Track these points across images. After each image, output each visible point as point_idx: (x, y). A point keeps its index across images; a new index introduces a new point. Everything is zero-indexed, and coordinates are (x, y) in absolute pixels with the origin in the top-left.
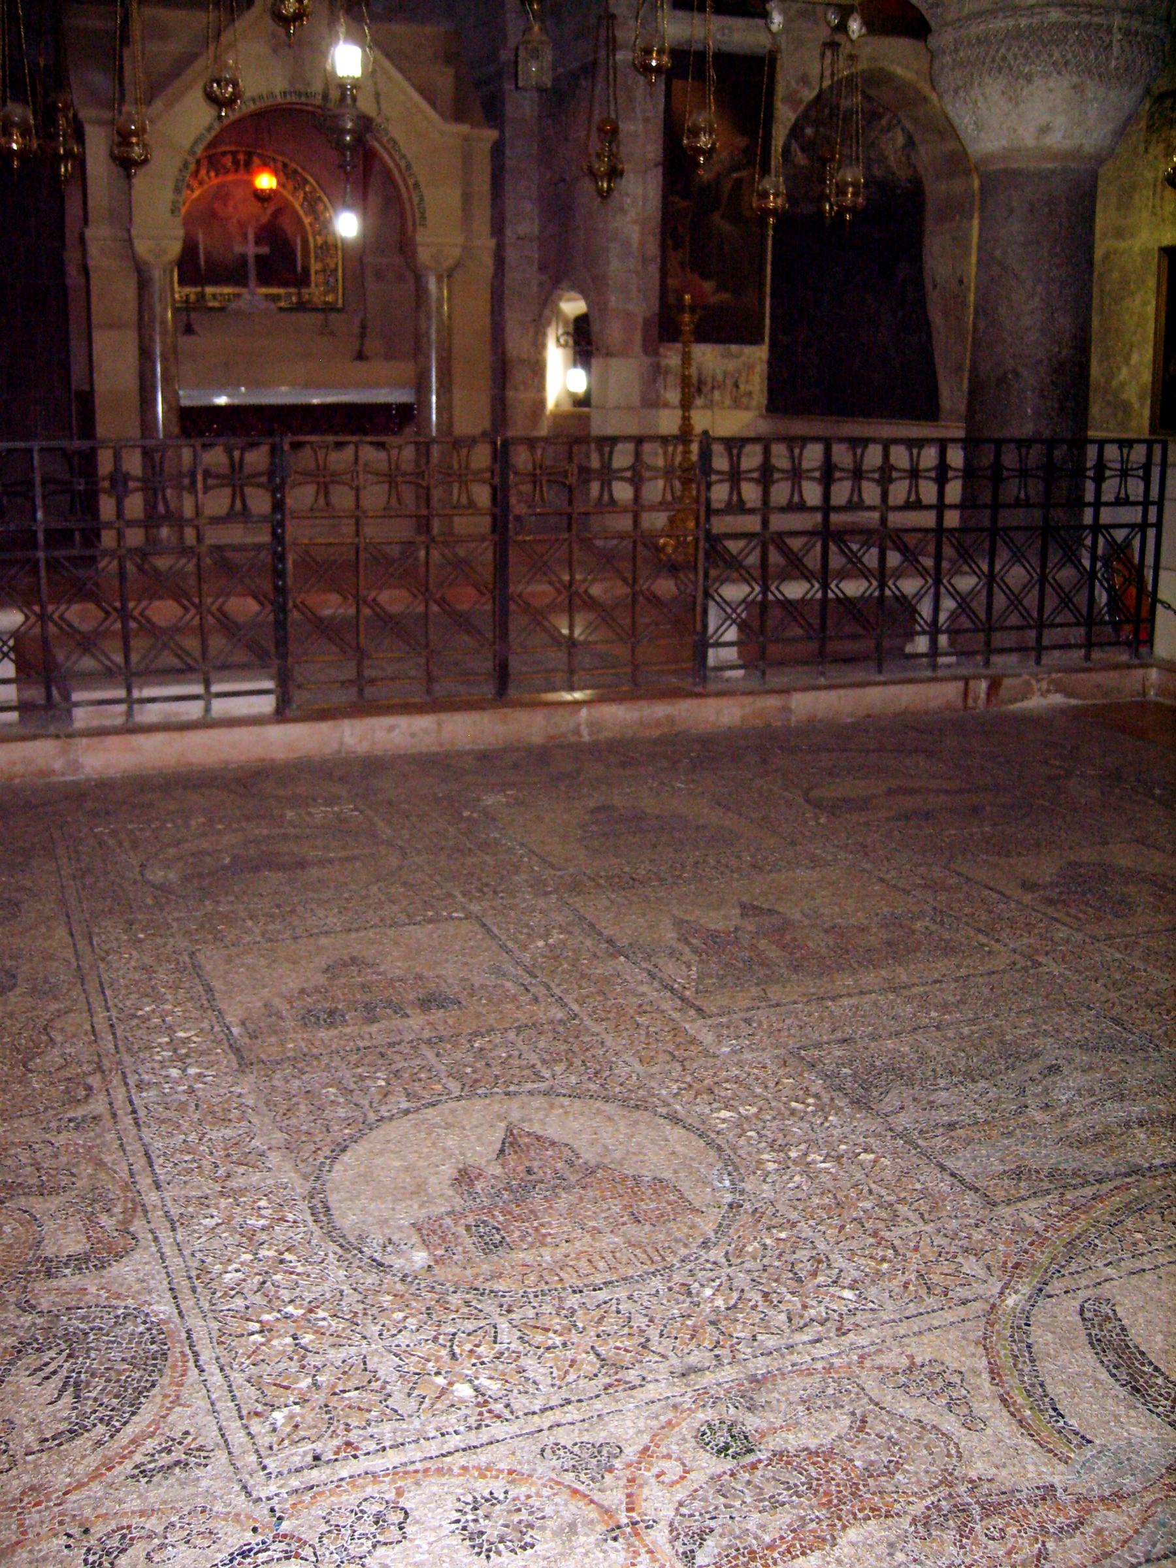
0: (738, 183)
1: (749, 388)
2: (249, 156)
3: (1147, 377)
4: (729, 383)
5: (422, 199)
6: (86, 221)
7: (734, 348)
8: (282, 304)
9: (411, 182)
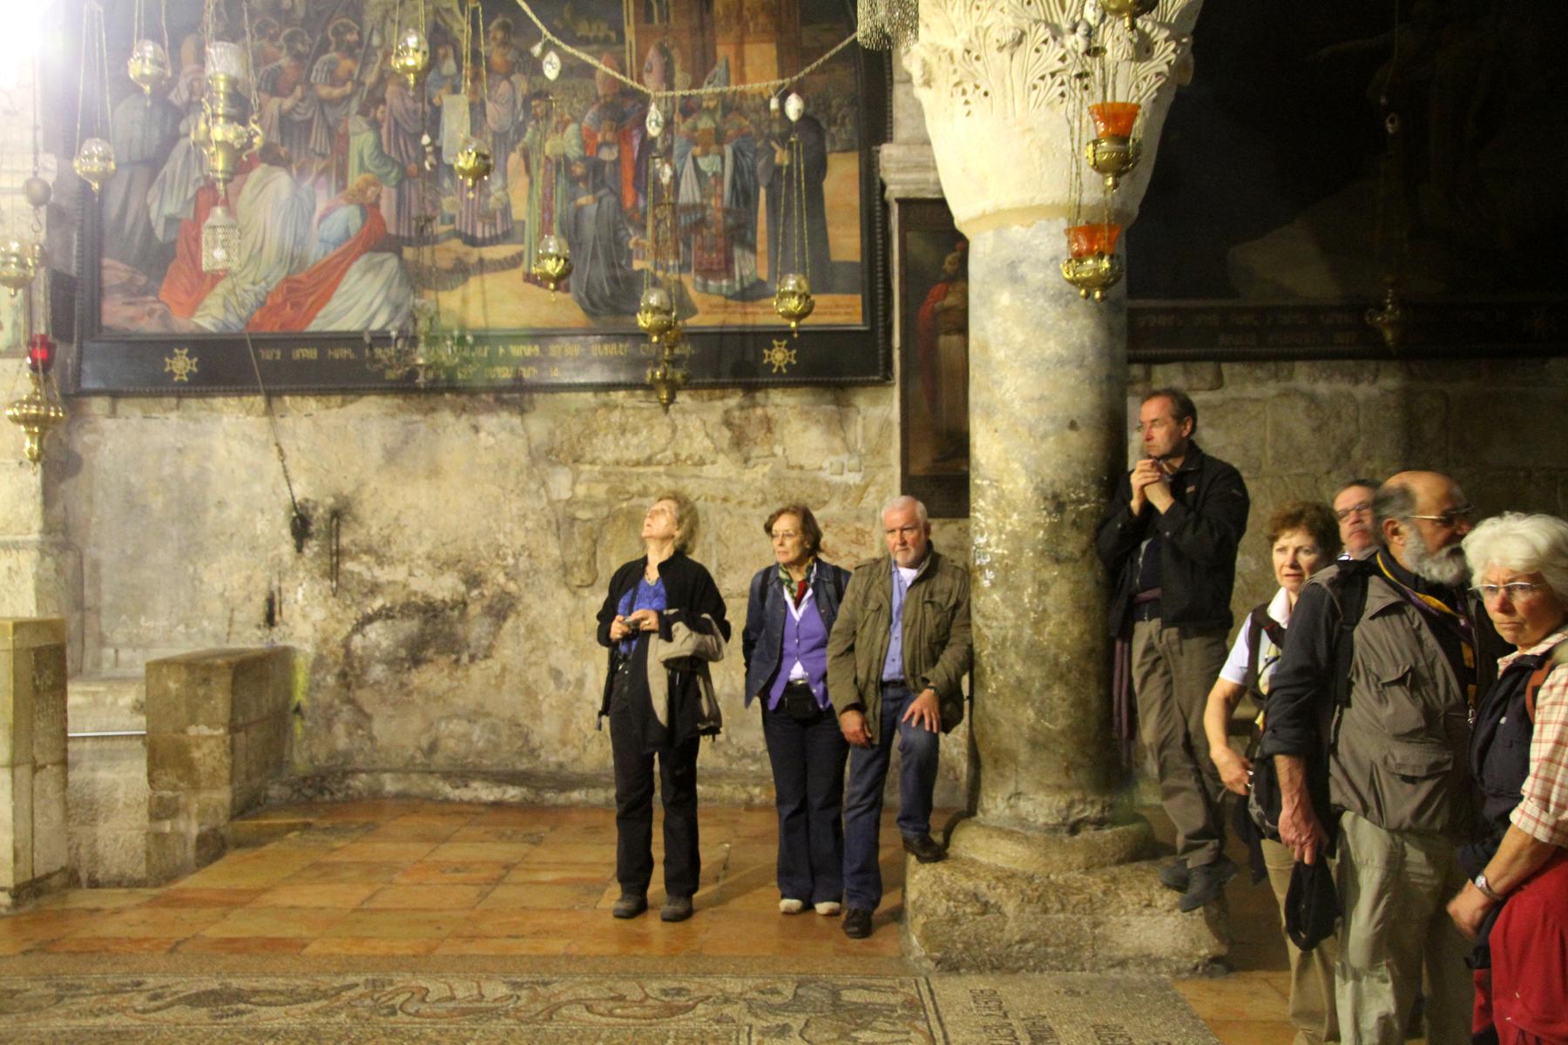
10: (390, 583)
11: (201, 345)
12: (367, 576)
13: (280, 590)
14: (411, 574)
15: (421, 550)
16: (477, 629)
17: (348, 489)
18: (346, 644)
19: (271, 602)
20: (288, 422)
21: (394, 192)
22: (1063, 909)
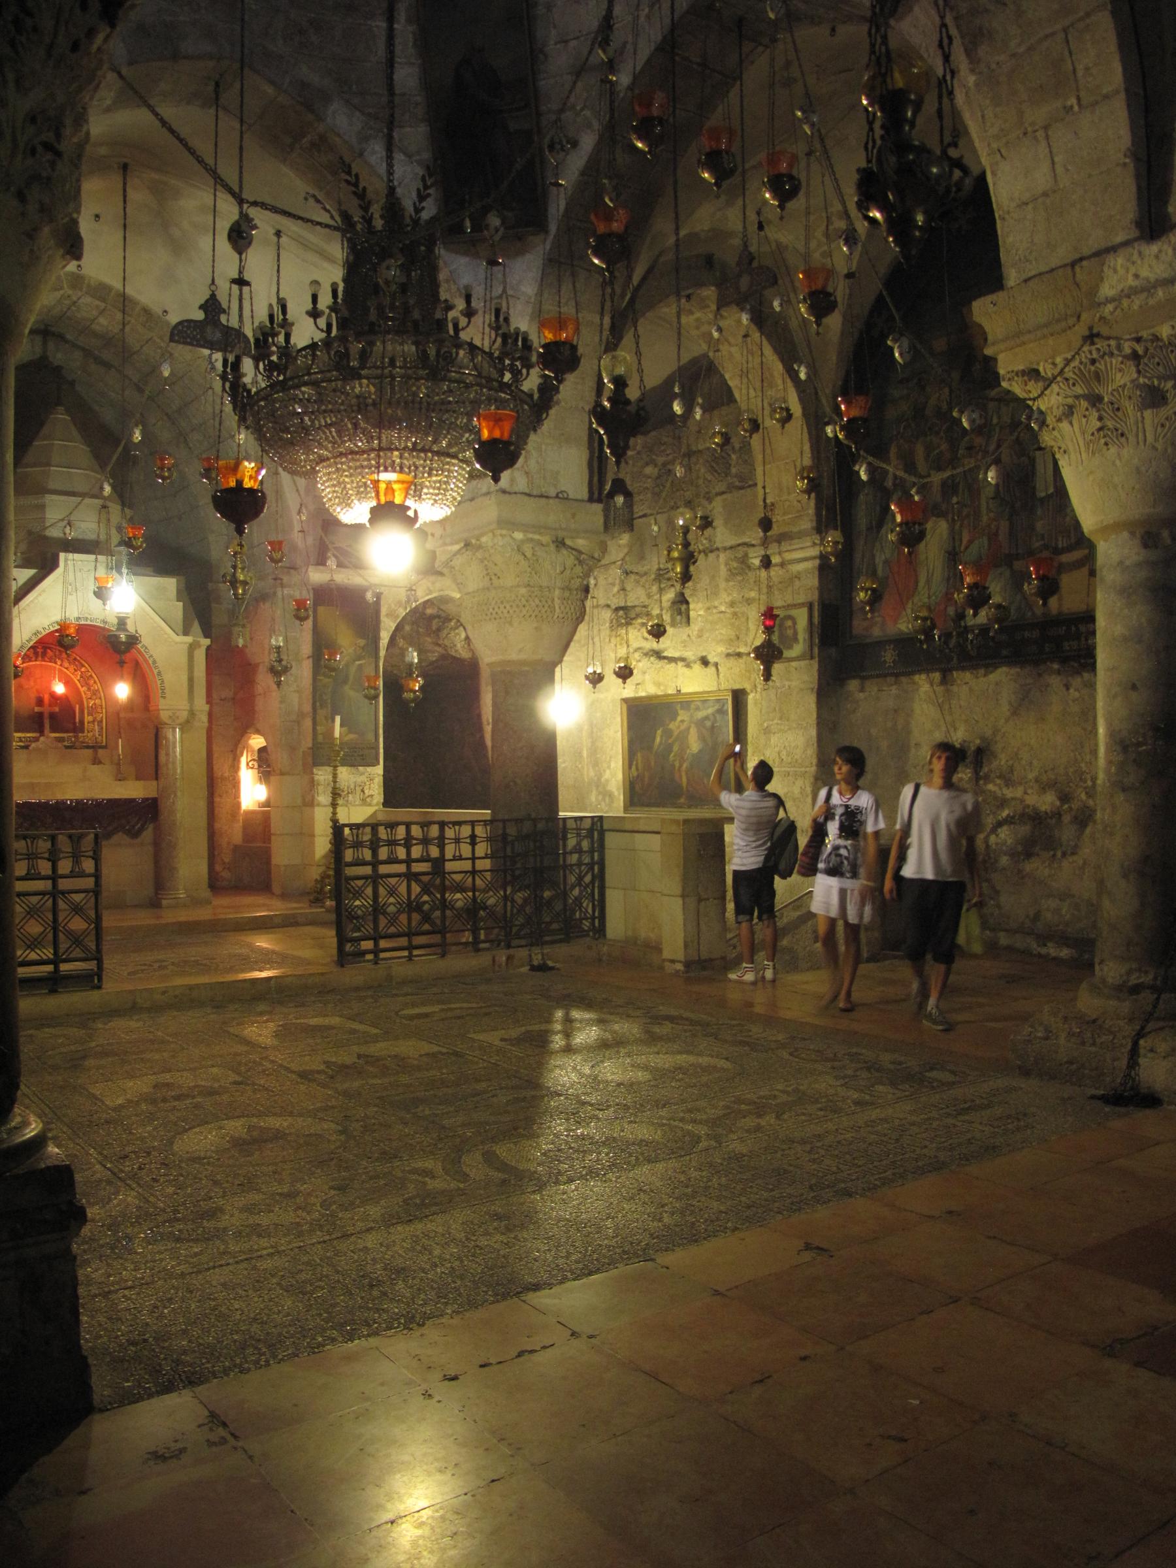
0: (360, 666)
1: (371, 792)
3: (620, 776)
8: (66, 743)
9: (155, 672)
10: (1013, 799)
11: (903, 643)
12: (999, 793)
14: (1026, 793)
15: (1031, 776)
16: (1067, 833)
17: (988, 733)
20: (955, 689)
21: (1007, 523)
22: (1094, 1044)
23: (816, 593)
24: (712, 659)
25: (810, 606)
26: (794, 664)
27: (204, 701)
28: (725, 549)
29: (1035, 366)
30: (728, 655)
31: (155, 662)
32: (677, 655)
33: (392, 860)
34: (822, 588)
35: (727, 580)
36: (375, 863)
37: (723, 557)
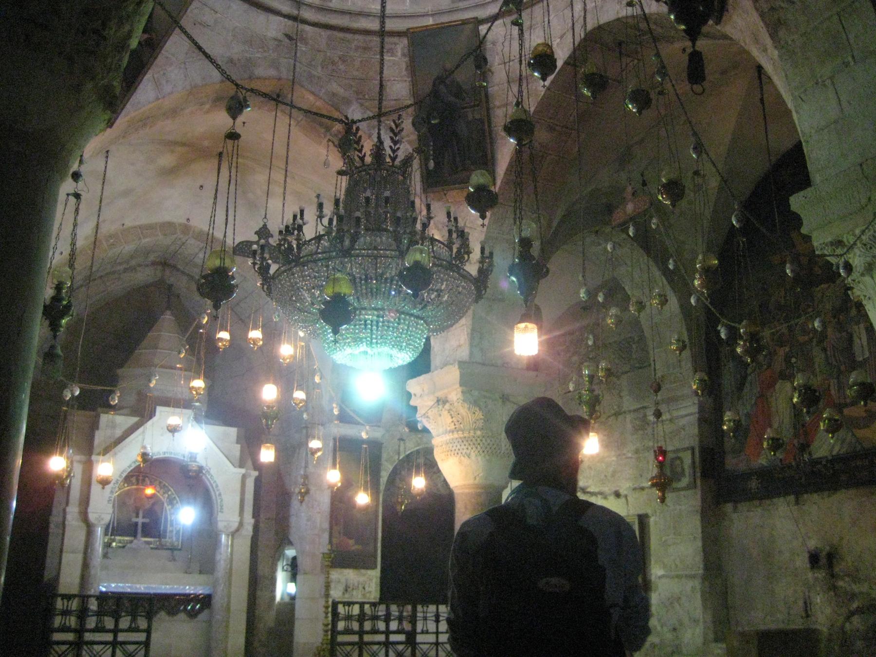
1: (370, 589)
2: (145, 477)
4: (361, 587)
5: (222, 501)
6: (67, 504)
7: (363, 571)
8: (152, 546)
11: (764, 474)
12: (848, 589)
13: (809, 597)
14: (871, 588)
18: (842, 627)
19: (805, 603)
20: (806, 508)
23: (697, 439)
24: (623, 492)
25: (693, 449)
26: (682, 493)
27: (251, 516)
28: (630, 411)
29: (840, 239)
30: (634, 489)
31: (217, 486)
32: (597, 490)
33: (375, 632)
34: (701, 434)
35: (632, 434)
36: (361, 633)
37: (629, 417)
